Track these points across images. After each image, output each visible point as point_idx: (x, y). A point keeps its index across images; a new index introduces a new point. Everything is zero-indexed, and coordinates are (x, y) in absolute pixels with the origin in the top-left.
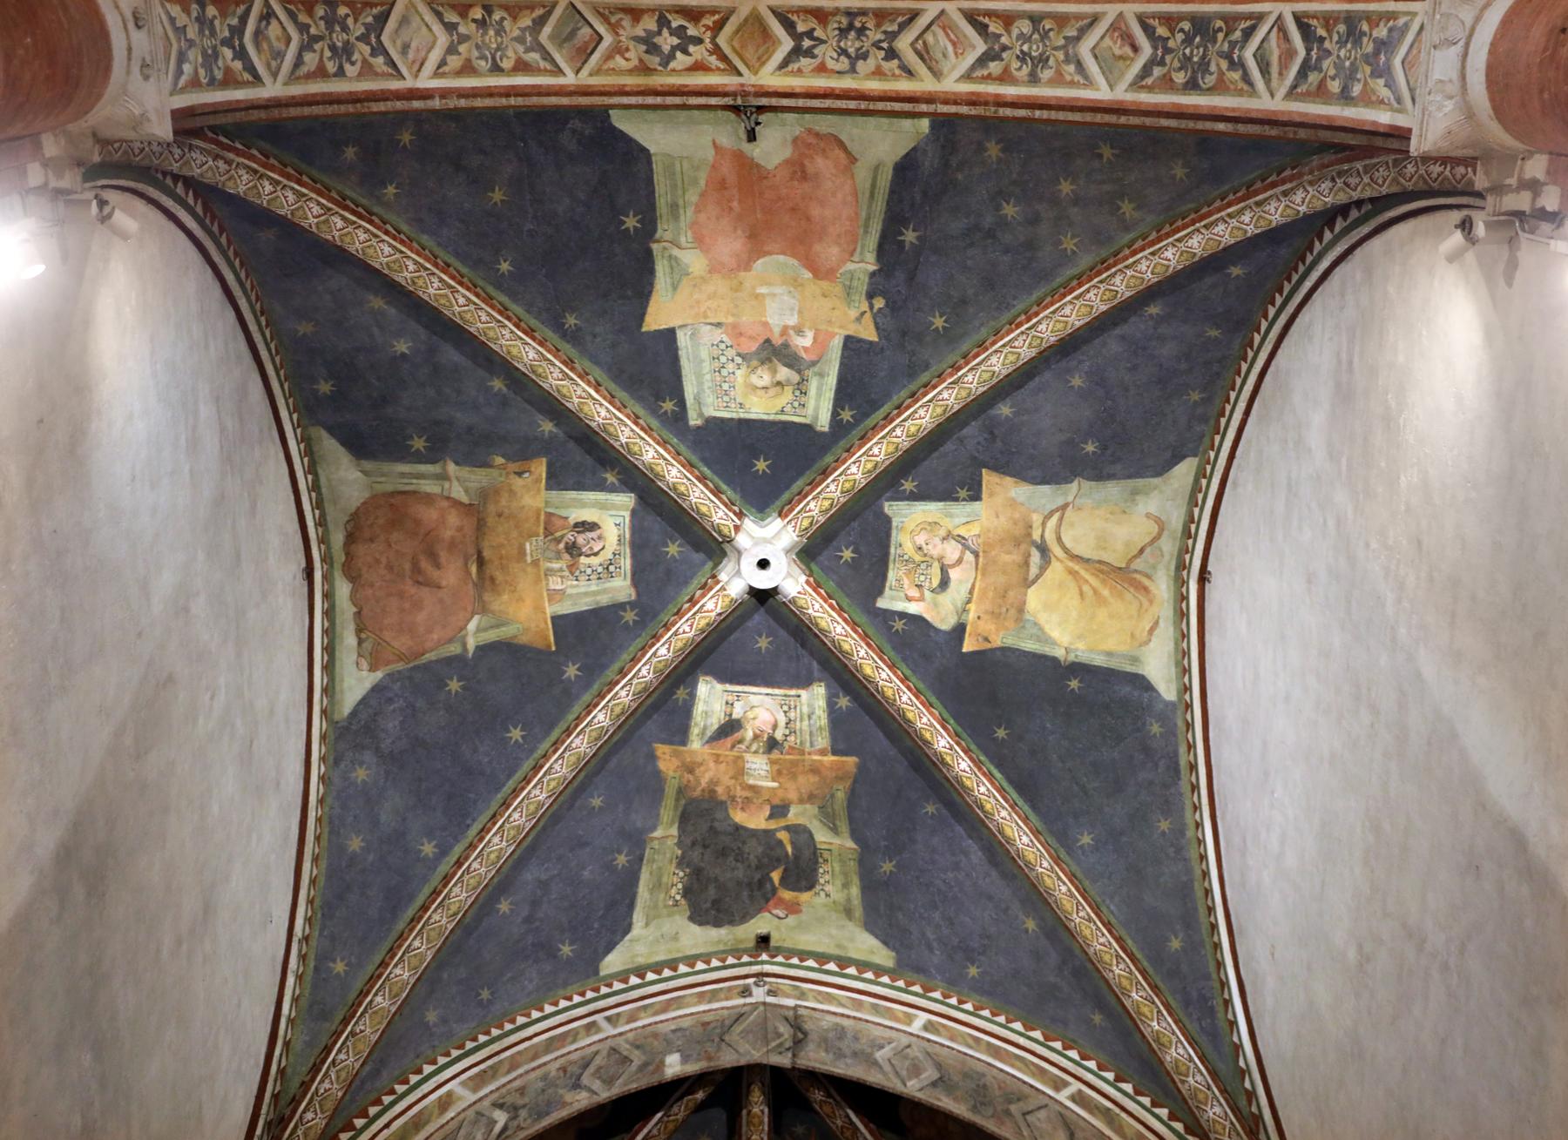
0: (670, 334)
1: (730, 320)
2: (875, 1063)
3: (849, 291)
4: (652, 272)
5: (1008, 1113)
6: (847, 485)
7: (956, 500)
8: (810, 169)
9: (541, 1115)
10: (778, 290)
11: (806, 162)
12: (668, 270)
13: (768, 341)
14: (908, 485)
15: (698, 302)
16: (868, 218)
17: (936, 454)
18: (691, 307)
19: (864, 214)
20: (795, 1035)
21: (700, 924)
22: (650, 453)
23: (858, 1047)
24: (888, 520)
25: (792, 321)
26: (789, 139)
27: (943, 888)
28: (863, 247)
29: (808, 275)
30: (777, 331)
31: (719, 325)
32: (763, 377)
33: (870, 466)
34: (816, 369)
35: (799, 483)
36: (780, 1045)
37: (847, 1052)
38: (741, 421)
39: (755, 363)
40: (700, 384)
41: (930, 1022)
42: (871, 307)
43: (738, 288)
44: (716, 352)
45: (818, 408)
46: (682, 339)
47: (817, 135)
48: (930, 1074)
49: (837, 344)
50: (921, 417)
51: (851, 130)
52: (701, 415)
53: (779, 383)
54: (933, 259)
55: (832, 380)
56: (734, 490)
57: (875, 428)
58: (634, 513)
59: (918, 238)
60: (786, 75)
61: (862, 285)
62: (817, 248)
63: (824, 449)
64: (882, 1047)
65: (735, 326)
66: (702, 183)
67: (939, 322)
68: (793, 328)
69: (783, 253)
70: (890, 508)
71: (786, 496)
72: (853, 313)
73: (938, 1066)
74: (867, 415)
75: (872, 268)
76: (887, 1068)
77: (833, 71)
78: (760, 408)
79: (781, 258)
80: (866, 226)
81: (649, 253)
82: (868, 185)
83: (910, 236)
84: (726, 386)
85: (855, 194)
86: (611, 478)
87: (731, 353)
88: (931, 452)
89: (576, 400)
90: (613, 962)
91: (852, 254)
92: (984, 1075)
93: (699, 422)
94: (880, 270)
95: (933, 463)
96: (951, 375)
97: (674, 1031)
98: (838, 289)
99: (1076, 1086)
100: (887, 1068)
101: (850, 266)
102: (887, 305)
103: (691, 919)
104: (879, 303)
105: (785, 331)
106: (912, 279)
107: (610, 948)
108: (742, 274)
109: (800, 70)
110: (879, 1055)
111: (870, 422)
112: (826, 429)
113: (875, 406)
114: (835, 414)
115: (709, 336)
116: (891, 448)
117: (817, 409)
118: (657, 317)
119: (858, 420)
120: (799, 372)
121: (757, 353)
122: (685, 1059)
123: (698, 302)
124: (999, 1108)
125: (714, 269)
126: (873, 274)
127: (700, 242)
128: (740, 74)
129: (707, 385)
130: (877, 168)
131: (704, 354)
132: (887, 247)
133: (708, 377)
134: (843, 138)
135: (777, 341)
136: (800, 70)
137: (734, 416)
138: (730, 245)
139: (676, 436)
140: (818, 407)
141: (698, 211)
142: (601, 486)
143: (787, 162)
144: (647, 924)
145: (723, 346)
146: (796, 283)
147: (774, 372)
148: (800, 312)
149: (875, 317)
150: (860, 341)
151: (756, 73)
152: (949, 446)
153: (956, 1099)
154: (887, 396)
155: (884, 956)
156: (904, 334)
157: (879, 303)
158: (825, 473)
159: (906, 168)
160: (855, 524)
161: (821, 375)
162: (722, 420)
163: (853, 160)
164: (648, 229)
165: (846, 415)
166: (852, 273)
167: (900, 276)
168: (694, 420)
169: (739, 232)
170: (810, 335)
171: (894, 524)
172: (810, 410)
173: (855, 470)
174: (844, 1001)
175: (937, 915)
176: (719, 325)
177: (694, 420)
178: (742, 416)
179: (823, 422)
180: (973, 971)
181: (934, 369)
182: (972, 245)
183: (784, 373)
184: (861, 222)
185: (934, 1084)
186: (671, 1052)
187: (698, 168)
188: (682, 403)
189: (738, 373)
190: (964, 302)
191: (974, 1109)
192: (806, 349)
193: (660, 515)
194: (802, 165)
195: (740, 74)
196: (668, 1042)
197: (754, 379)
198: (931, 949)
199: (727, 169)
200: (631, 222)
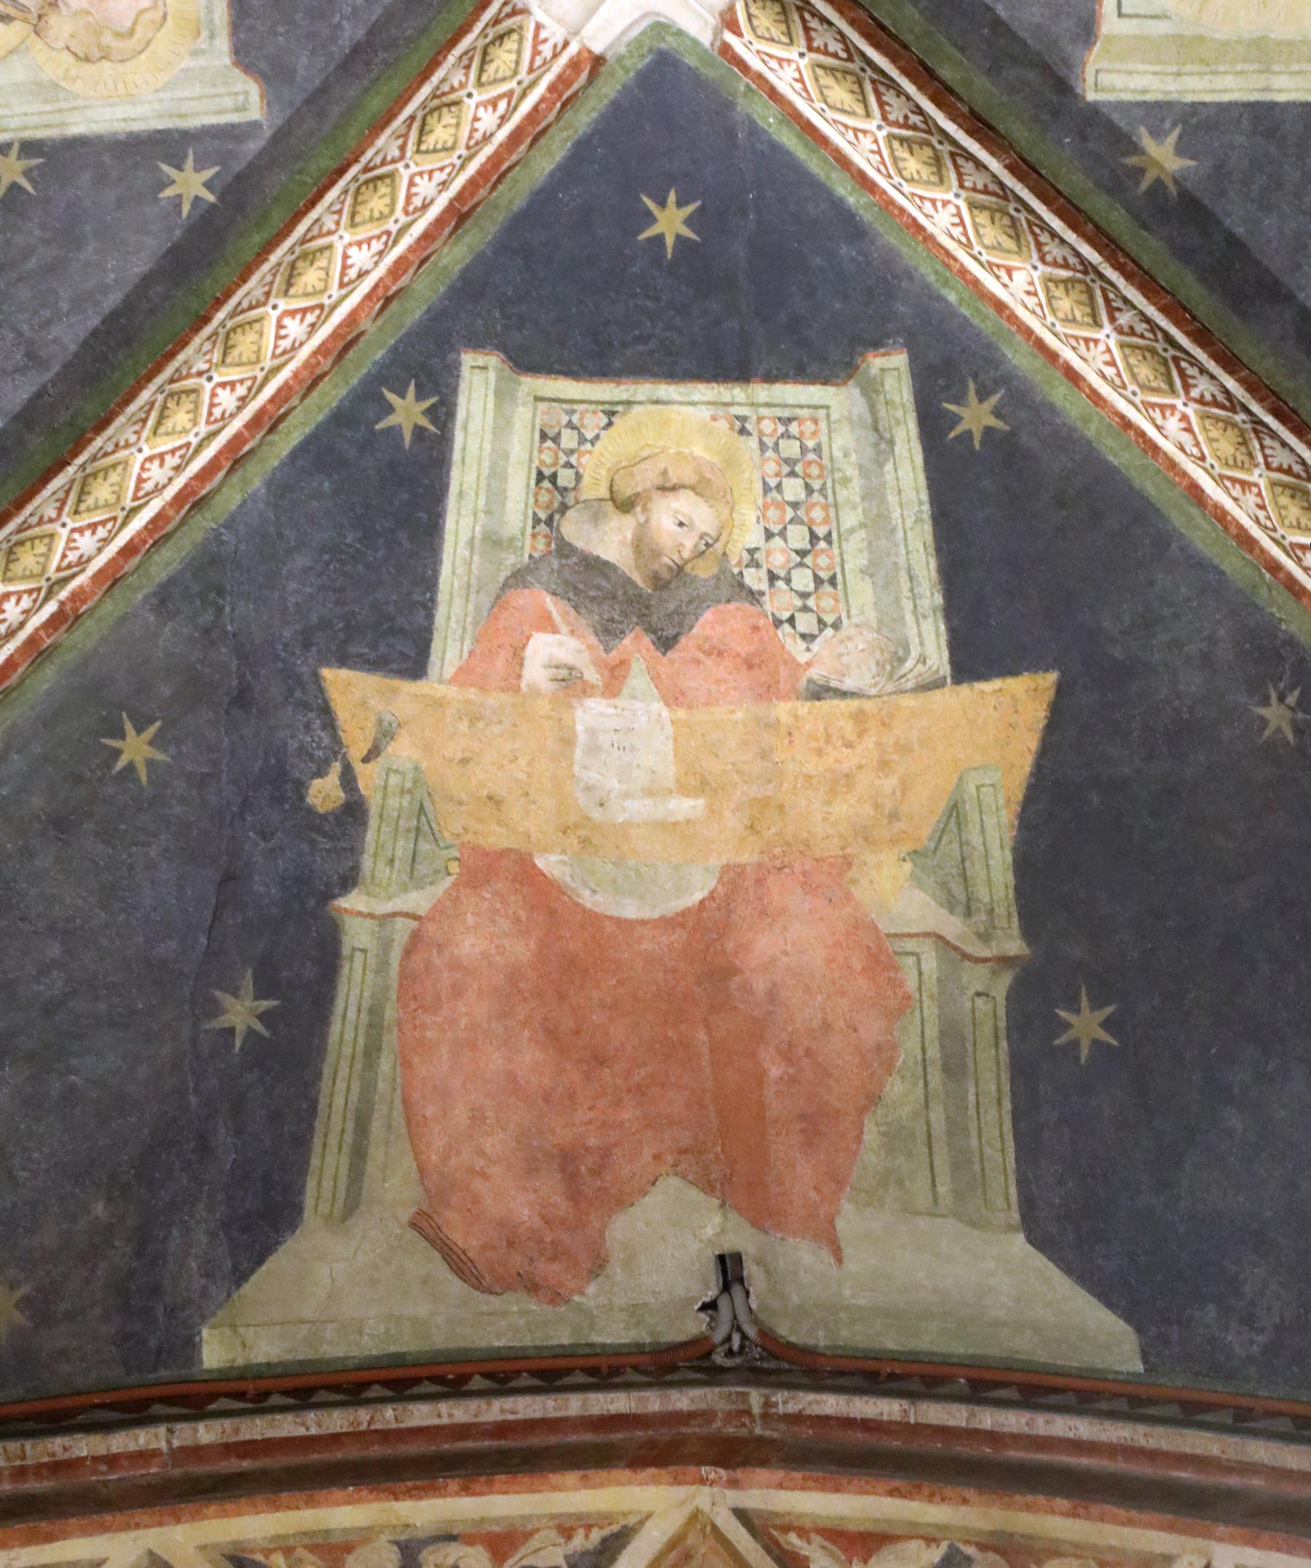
0: (973, 657)
1: (782, 710)
3: (421, 822)
4: (1024, 865)
6: (376, 203)
7: (29, 148)
8: (551, 1187)
10: (639, 809)
11: (562, 1206)
12: (976, 870)
13: (666, 643)
14: (191, 185)
15: (884, 765)
16: (372, 1052)
17: (113, 300)
18: (904, 749)
19: (385, 1065)
22: (1018, 284)
24: (244, 56)
25: (592, 713)
26: (616, 1269)
28: (383, 965)
29: (549, 863)
30: (638, 679)
31: (819, 692)
32: (676, 523)
33: (310, 277)
34: (511, 561)
35: (546, 162)
38: (740, 372)
39: (704, 571)
40: (873, 495)
42: (348, 779)
43: (760, 812)
44: (825, 602)
45: (498, 425)
46: (931, 645)
47: (533, 1288)
49: (449, 650)
50: (155, 457)
51: (440, 1315)
52: (871, 389)
53: (626, 506)
54: (167, 948)
55: (460, 526)
56: (755, 131)
57: (311, 380)
58: (1087, 30)
59: (215, 1009)
60: (607, 1518)
61: (380, 844)
62: (521, 950)
63: (471, 288)
65: (768, 692)
66: (871, 1135)
67: (136, 748)
68: (586, 690)
69: (620, 923)
70: (238, 100)
71: (584, 118)
72: (402, 751)
74: (341, 418)
75: (352, 902)
77: (469, 1540)
78: (681, 421)
79: (630, 910)
80: (375, 1026)
81: (1030, 929)
82: (376, 1153)
83: (241, 1012)
84: (794, 489)
85: (414, 1124)
86: (1164, 156)
87: (780, 602)
88: (128, 306)
89: (1258, 476)
91: (416, 938)
93: (874, 371)
94: (327, 896)
95: (119, 265)
96: (77, 596)
98: (453, 823)
101: (419, 901)
102: (300, 788)
104: (324, 792)
105: (614, 679)
106: (228, 878)
108: (748, 857)
109: (567, 1532)
111: (332, 394)
112: (469, 359)
113: (317, 452)
114: (443, 414)
115: (847, 657)
116: (244, 344)
117: (502, 428)
118: (1011, 713)
119: (368, 399)
120: (564, 549)
121: (699, 603)
123: (884, 765)
125: (832, 875)
126: (349, 881)
127: (880, 956)
128: (742, 1515)
129: (852, 493)
130: (352, 1205)
131: (862, 594)
132: (310, 972)
133: (850, 519)
134: (456, 1286)
135: (636, 645)
136: (567, 1532)
137: (762, 392)
138: (789, 947)
139: (950, 311)
140: (498, 425)
141: (884, 1054)
142: (1199, 123)
143: (622, 1202)
145: (806, 623)
146: (586, 835)
147: (642, 545)
148: (568, 741)
149: (337, 747)
150: (376, 664)
151: (695, 1516)
152: (68, 335)
154: (280, 489)
156: (242, 699)
157: (324, 792)
158: (459, 215)
159: (263, 1215)
160: (351, 33)
161: (494, 542)
162: (801, 374)
163: (424, 1226)
164: (1034, 998)
165: (407, 412)
166: (414, 879)
167: (264, 886)
168: (891, 368)
169: (760, 985)
170: (535, 672)
171: (223, 43)
172: (524, 418)
173: (352, 257)
176: (819, 692)
177: (891, 368)
178: (737, 393)
179: (479, 379)
181: (139, 591)
182: (48, 1009)
183: (610, 542)
184: (390, 1040)
187: (887, 1178)
188: (933, 426)
189: (754, 537)
190: (61, 825)
192: (546, 624)
193: (997, 23)
194: (574, 1195)
195: (742, 1515)
197: (703, 516)
199: (800, 1175)
200: (1086, 1025)
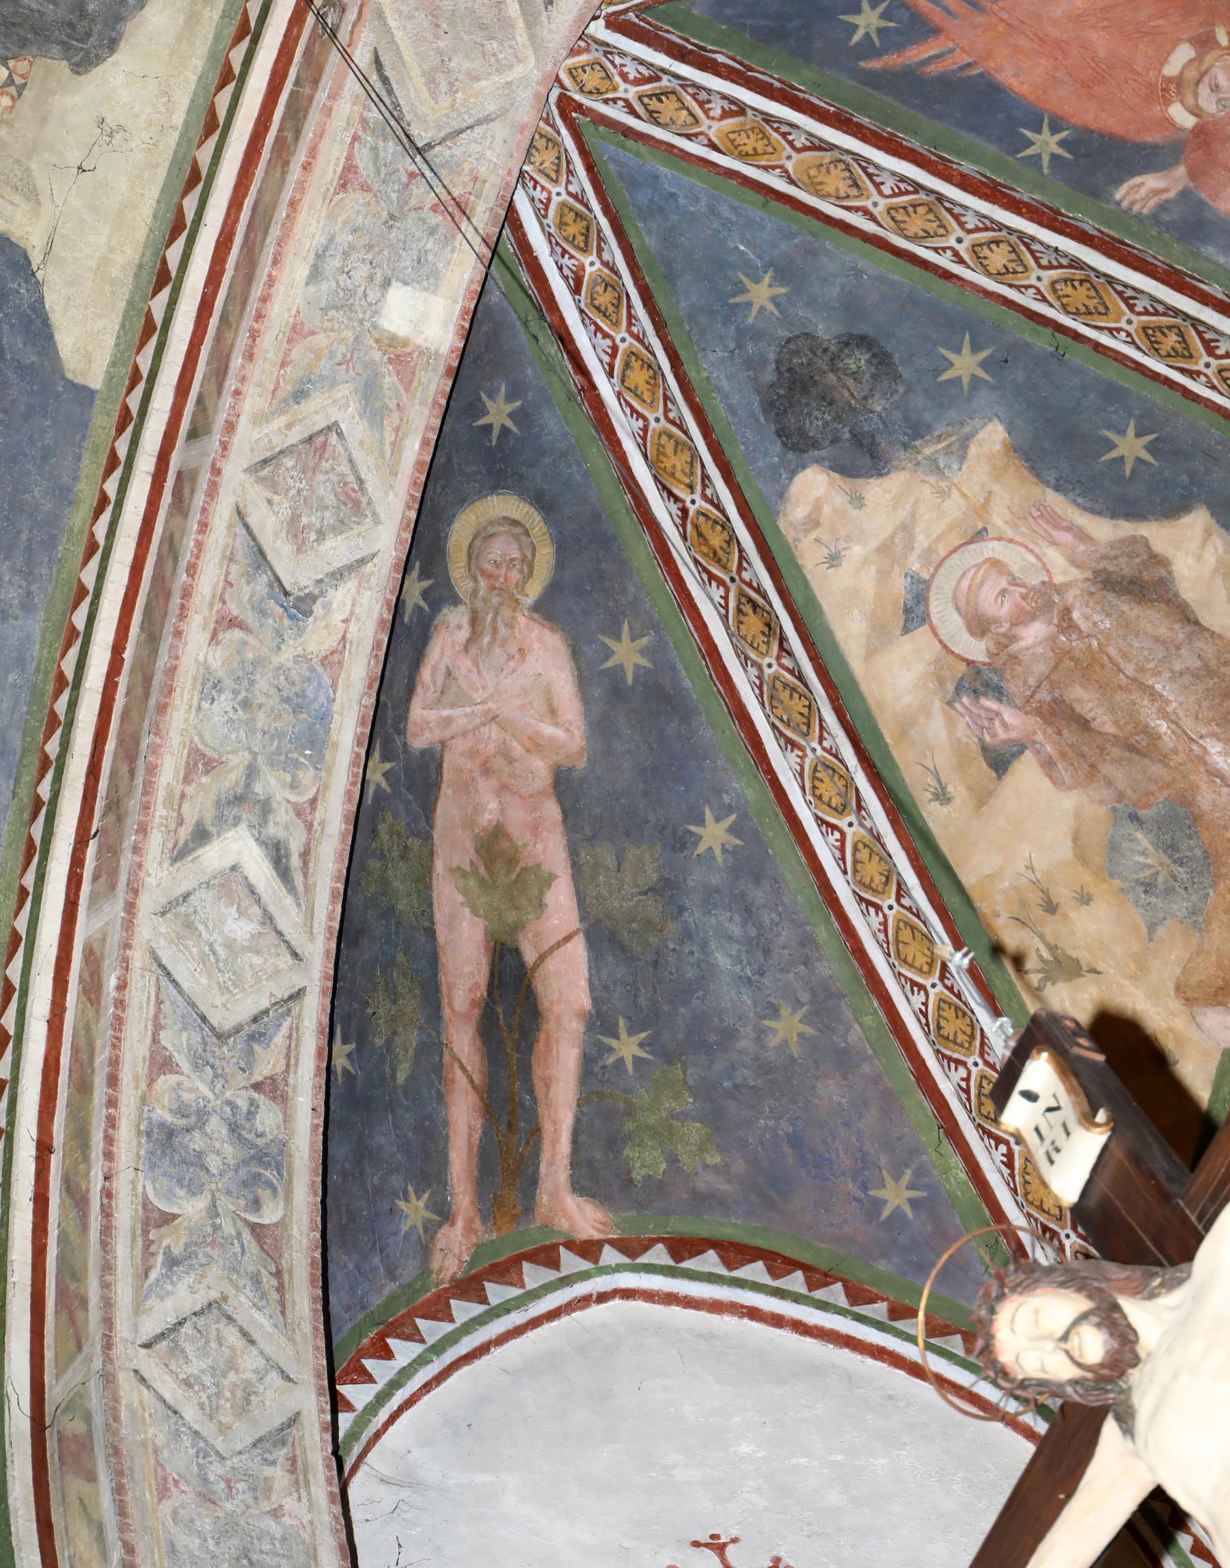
9: (315, 741)
21: (112, 45)
90: (86, 339)
97: (315, 274)
103: (83, 64)
107: (38, 328)
122: (425, 275)
144: (32, 194)
186: (375, 308)
196: (343, 302)
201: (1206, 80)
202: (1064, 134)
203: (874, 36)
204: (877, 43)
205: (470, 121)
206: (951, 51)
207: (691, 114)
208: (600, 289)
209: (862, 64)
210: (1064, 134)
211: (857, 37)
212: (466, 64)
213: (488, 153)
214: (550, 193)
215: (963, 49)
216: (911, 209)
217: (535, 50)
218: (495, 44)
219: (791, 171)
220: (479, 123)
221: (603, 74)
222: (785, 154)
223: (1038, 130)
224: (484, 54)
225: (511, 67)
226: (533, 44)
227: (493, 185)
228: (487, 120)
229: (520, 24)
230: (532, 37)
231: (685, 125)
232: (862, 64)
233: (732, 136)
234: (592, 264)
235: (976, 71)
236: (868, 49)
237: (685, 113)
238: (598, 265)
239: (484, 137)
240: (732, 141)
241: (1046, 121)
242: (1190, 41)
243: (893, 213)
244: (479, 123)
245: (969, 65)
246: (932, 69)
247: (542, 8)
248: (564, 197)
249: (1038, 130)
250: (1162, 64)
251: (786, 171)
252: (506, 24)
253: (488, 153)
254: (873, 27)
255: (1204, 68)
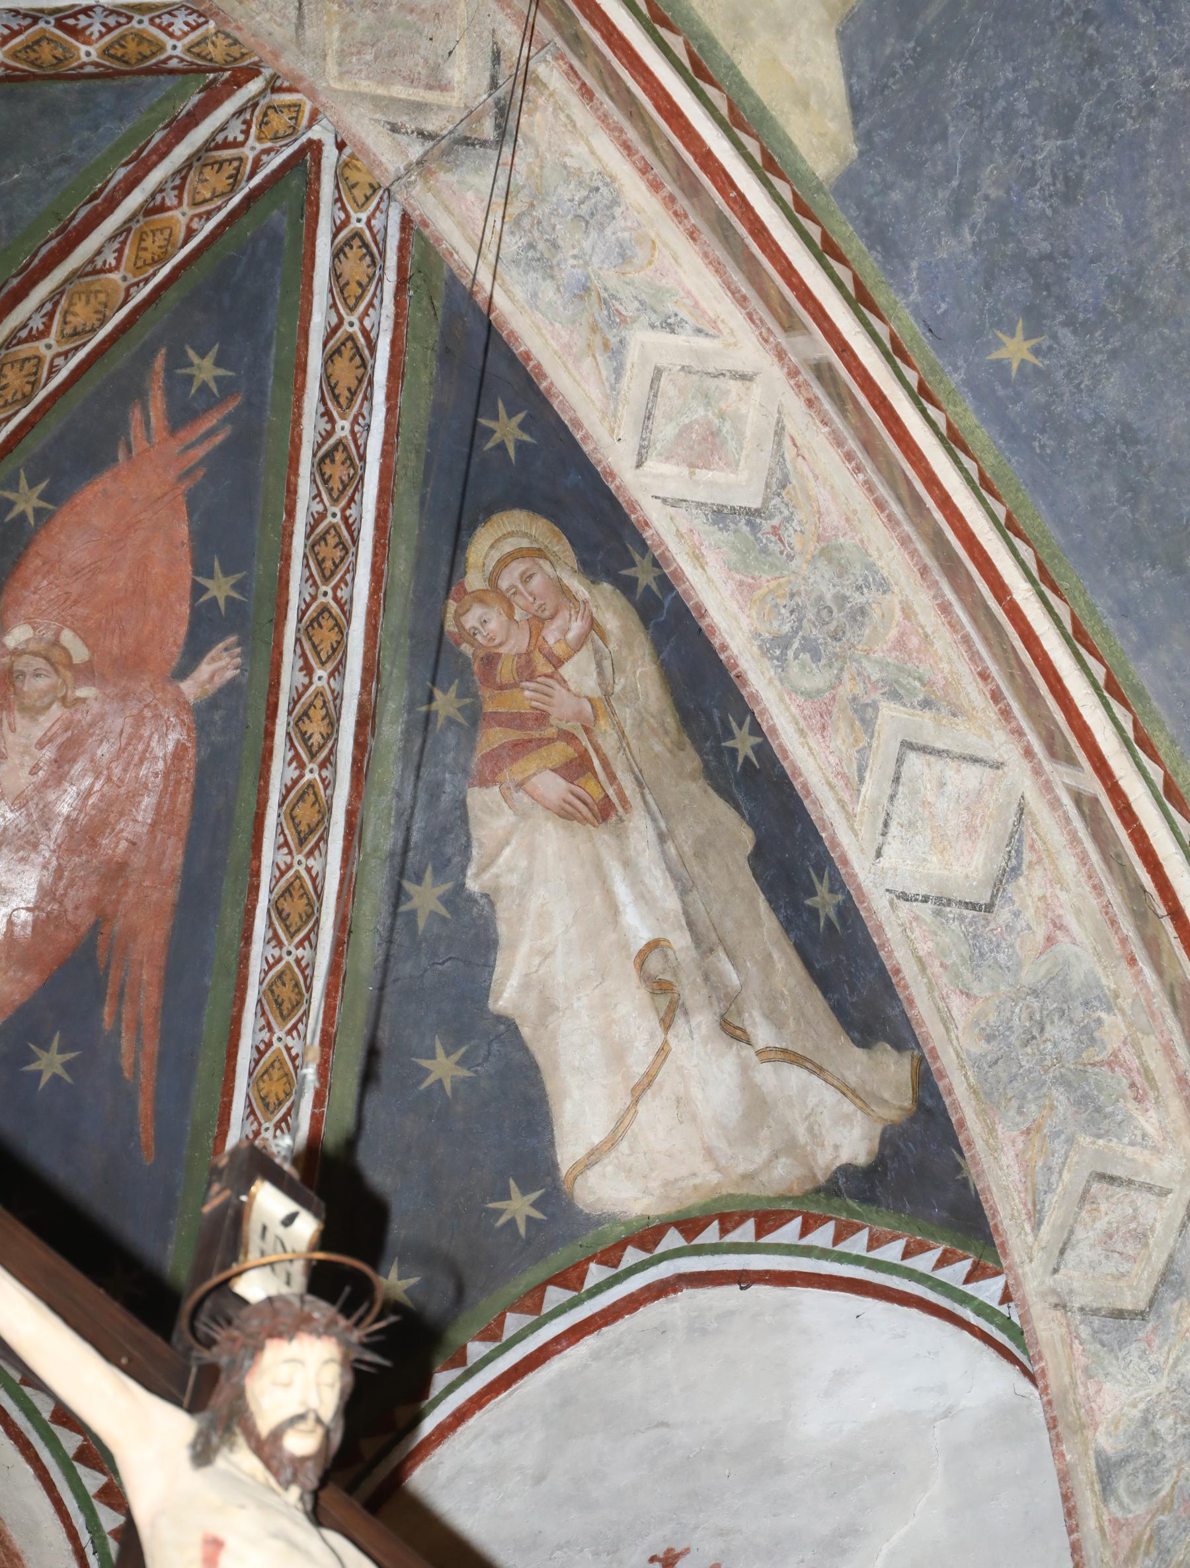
2: (615, 352)
5: (864, 715)
20: (472, 115)
23: (608, 277)
27: (1130, 93)
36: (419, 107)
37: (569, 269)
41: (830, 367)
48: (741, 485)
64: (670, 326)
73: (780, 483)
76: (634, 386)
92: (884, 586)
99: (1095, 787)
100: (634, 386)
110: (645, 344)
124: (847, 689)
153: (746, 589)
155: (820, 136)
174: (660, 144)
175: (1051, 147)
180: (1015, 349)
185: (720, 515)
191: (776, 648)
198: (959, 211)
201: (48, 667)
202: (32, 520)
203: (188, 371)
204: (179, 371)
205: (306, 9)
206: (149, 439)
207: (205, 201)
208: (59, 52)
209: (163, 351)
210: (32, 520)
211: (191, 353)
212: (362, 24)
213: (267, 16)
214: (179, 39)
215: (145, 451)
216: (32, 379)
217: (347, 93)
218: (369, 57)
219: (111, 276)
220: (301, 16)
221: (281, 133)
222: (130, 276)
223: (42, 497)
224: (364, 44)
225: (340, 65)
226: (355, 94)
227: (233, 10)
228: (300, 25)
229: (381, 91)
230: (363, 96)
231: (195, 192)
232: (163, 351)
233: (167, 232)
234: (88, 54)
235: (121, 456)
236: (177, 360)
237: (208, 195)
238: (84, 59)
239: (284, 16)
240: (162, 231)
241: (50, 507)
242: (90, 661)
243: (34, 361)
244: (301, 16)
245: (130, 451)
246: (136, 415)
247: (391, 119)
248: (169, 52)
249: (42, 497)
250: (74, 631)
251: (110, 270)
252: (385, 78)
253: (267, 16)
254: (196, 372)
255: (60, 668)
